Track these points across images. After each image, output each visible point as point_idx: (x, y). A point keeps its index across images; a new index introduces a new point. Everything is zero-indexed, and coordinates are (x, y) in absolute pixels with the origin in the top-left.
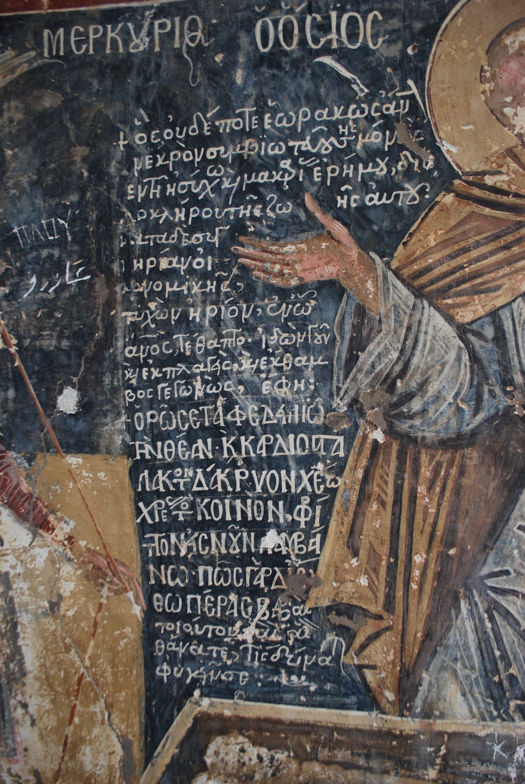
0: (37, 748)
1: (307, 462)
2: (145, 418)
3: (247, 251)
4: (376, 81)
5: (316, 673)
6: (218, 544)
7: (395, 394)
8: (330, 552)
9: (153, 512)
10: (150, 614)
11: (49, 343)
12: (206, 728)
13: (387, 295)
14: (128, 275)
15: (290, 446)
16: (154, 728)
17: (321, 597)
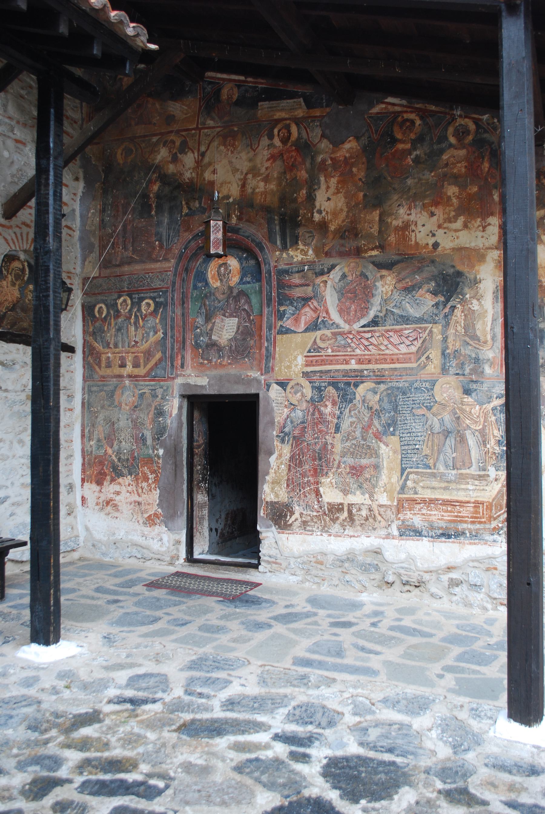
2: (401, 431)
3: (414, 410)
4: (428, 391)
6: (411, 447)
9: (402, 443)
10: (402, 457)
11: (389, 422)
13: (429, 415)
15: (419, 434)
16: (402, 475)
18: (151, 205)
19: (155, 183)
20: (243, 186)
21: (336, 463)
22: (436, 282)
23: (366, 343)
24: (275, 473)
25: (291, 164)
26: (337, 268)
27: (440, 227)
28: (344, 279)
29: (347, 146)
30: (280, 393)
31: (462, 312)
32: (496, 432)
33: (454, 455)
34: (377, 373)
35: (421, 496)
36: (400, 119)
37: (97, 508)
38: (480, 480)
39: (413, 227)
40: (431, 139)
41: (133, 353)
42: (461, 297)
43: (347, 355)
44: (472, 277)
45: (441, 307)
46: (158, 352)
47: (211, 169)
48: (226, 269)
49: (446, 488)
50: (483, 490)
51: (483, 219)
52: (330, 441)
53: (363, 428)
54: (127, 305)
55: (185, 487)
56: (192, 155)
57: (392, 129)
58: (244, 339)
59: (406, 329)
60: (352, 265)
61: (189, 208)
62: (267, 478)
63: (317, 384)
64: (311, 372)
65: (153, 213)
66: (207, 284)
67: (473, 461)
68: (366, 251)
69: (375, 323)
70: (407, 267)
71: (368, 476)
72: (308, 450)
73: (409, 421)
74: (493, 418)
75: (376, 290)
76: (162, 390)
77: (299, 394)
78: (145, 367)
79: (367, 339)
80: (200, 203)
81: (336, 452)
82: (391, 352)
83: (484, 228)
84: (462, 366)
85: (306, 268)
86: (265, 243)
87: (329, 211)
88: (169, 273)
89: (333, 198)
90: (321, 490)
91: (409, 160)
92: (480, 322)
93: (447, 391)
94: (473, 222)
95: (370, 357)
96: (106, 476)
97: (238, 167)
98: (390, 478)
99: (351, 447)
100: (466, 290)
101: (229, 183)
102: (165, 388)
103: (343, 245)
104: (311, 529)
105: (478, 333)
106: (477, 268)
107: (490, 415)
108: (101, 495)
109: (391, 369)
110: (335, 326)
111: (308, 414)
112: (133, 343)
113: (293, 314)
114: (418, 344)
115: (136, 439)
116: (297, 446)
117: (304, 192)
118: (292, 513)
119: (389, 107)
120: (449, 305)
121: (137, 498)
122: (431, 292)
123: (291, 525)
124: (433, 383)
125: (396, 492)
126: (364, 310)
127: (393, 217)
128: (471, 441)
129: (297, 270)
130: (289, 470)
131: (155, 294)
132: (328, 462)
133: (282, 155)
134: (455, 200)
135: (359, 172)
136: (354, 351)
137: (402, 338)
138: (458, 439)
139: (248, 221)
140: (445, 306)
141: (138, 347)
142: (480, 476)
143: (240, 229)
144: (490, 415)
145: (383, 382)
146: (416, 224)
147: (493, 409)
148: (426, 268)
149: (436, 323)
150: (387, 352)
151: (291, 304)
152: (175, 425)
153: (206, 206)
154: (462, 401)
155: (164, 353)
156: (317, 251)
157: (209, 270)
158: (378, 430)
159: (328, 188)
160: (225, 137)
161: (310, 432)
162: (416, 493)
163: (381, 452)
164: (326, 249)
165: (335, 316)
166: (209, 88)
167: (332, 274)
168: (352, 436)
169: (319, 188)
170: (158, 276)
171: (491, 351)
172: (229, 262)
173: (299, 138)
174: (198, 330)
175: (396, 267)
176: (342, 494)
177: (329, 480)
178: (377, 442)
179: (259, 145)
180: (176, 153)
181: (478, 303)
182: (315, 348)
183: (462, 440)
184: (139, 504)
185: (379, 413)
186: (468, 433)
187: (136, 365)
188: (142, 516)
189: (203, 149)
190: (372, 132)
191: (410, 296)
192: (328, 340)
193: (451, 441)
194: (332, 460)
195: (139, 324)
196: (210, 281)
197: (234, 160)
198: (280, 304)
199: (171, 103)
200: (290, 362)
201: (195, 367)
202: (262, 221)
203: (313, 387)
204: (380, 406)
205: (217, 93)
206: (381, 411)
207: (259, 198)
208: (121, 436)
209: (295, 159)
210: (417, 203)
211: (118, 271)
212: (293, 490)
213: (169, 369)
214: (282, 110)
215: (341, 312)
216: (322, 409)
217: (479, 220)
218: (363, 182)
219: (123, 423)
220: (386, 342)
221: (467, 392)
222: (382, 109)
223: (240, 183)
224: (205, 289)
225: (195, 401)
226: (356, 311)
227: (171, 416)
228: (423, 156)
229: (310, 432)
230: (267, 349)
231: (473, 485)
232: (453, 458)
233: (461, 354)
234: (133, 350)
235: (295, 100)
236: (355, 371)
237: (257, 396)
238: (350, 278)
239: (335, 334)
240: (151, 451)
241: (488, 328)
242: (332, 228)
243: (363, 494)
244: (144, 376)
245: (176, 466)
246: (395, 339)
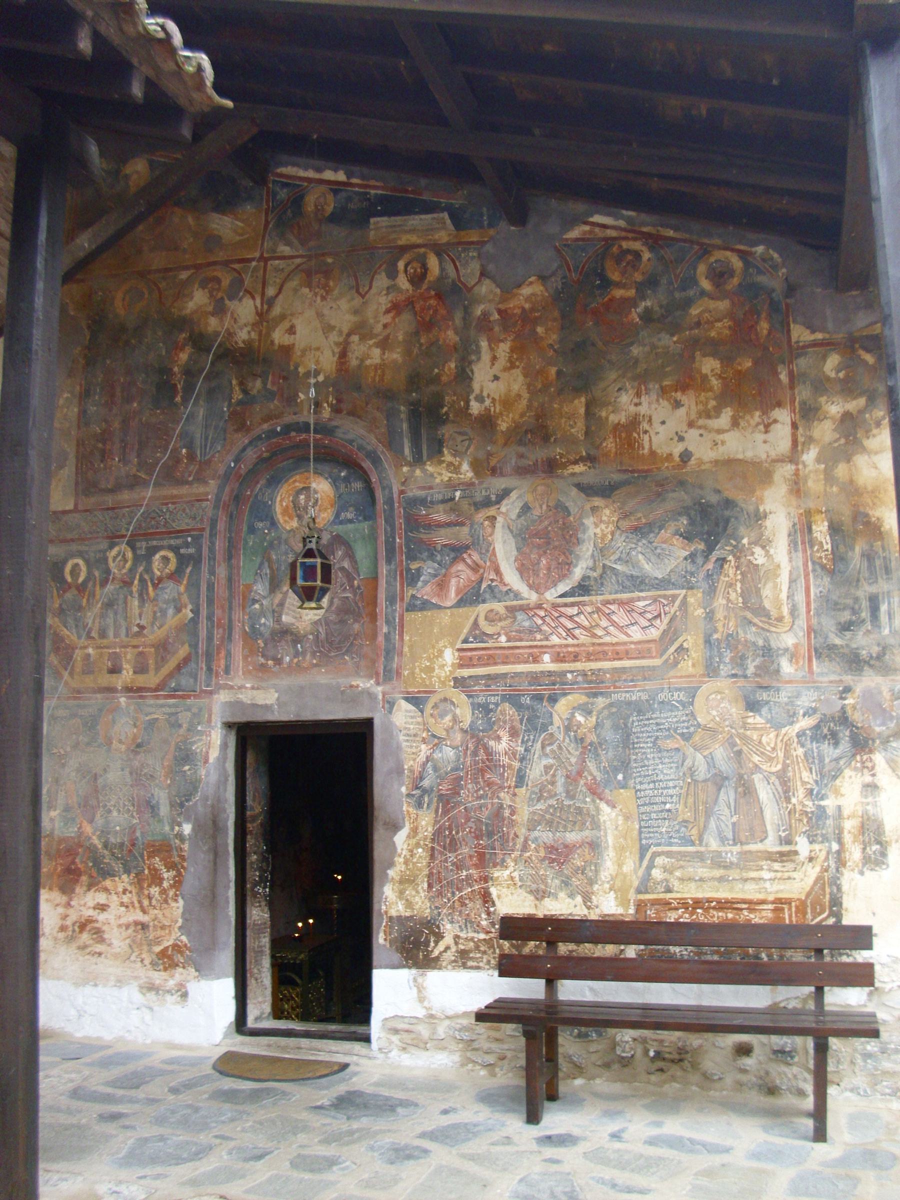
0: (611, 867)
1: (675, 787)
3: (659, 742)
5: (680, 838)
6: (656, 808)
7: (692, 771)
8: (680, 807)
10: (640, 827)
11: (615, 763)
12: (656, 855)
14: (634, 748)
16: (642, 858)
17: (680, 819)
18: (175, 385)
19: (182, 349)
20: (343, 355)
21: (521, 839)
22: (689, 515)
23: (570, 625)
24: (406, 863)
25: (427, 319)
26: (514, 495)
27: (691, 425)
29: (526, 291)
30: (412, 717)
31: (737, 568)
32: (806, 775)
33: (735, 819)
35: (679, 896)
36: (615, 249)
37: (61, 935)
38: (782, 861)
39: (645, 426)
40: (670, 283)
41: (135, 647)
42: (734, 543)
43: (536, 647)
44: (751, 508)
45: (700, 560)
46: (183, 644)
47: (286, 325)
48: (308, 498)
49: (721, 879)
50: (789, 878)
51: (765, 413)
52: (507, 801)
53: (567, 777)
54: (126, 561)
55: (231, 893)
56: (251, 302)
57: (602, 265)
58: (342, 622)
59: (639, 599)
60: (540, 489)
61: (245, 392)
62: (391, 873)
63: (481, 700)
64: (470, 677)
65: (178, 399)
66: (274, 524)
67: (769, 827)
68: (564, 466)
69: (583, 588)
71: (579, 863)
72: (468, 819)
73: (651, 762)
74: (800, 751)
75: (584, 532)
76: (189, 714)
77: (448, 717)
78: (156, 673)
79: (571, 618)
80: (265, 383)
81: (519, 820)
82: (615, 640)
83: (767, 428)
84: (740, 661)
85: (458, 494)
86: (383, 452)
87: (497, 398)
88: (204, 504)
89: (504, 376)
90: (494, 891)
91: (635, 316)
92: (770, 585)
93: (718, 706)
94: (748, 417)
95: (577, 649)
96: (80, 875)
97: (333, 323)
98: (620, 866)
99: (546, 811)
100: (742, 530)
101: (318, 349)
102: (194, 710)
103: (521, 456)
104: (475, 964)
105: (767, 604)
106: (758, 493)
107: (795, 745)
108: (71, 911)
109: (615, 670)
110: (512, 595)
111: (465, 754)
112: (136, 629)
113: (435, 576)
114: (662, 625)
115: (139, 806)
116: (446, 812)
117: (453, 365)
118: (439, 937)
119: (597, 230)
120: (713, 557)
121: (140, 916)
122: (681, 535)
123: (437, 958)
124: (692, 693)
125: (632, 891)
126: (564, 568)
127: (610, 408)
128: (765, 793)
129: (440, 497)
130: (432, 857)
131: (179, 542)
132: (504, 839)
133: (412, 303)
134: (715, 382)
135: (548, 333)
136: (547, 639)
137: (635, 615)
138: (740, 790)
139: (352, 413)
140: (706, 558)
141: (145, 636)
142: (782, 854)
143: (337, 427)
144: (795, 745)
145: (601, 693)
146: (650, 421)
147: (798, 735)
148: (671, 495)
149: (692, 588)
150: (607, 639)
151: (432, 557)
152: (214, 777)
153: (275, 389)
154: (745, 723)
155: (194, 646)
156: (476, 466)
157: (279, 499)
158: (594, 778)
159: (494, 359)
160: (309, 274)
161: (470, 786)
162: (669, 890)
163: (602, 819)
164: (492, 463)
165: (512, 578)
166: (283, 194)
168: (549, 791)
169: (479, 359)
170: (184, 510)
171: (791, 634)
172: (314, 485)
173: (442, 277)
174: (257, 606)
175: (618, 492)
176: (532, 898)
177: (507, 872)
178: (593, 801)
179: (370, 288)
180: (222, 298)
181: (763, 552)
183: (747, 791)
184: (144, 926)
185: (596, 748)
186: (757, 778)
187: (141, 669)
188: (150, 951)
189: (271, 292)
190: (569, 270)
191: (644, 541)
192: (500, 620)
193: (728, 795)
194: (512, 836)
195: (148, 594)
196: (280, 518)
197: (326, 311)
198: (412, 557)
199: (215, 216)
200: (429, 659)
201: (250, 672)
202: (378, 414)
203: (472, 704)
204: (598, 736)
205: (297, 201)
206: (600, 744)
207: (372, 374)
208: (109, 801)
209: (436, 311)
210: (651, 386)
211: (109, 500)
212: (440, 894)
213: (202, 676)
214: (412, 231)
215: (522, 570)
216: (492, 743)
217: (758, 413)
218: (555, 351)
219: (115, 775)
220: (604, 623)
221: (752, 706)
222: (585, 233)
223: (337, 350)
224: (269, 532)
225: (250, 736)
226: (549, 569)
227: (206, 761)
228: (656, 308)
229: (470, 786)
230: (387, 637)
231: (770, 870)
232: (734, 824)
233: (739, 641)
234: (135, 642)
235: (435, 215)
236: (550, 673)
237: (368, 723)
238: (537, 512)
239: (512, 610)
240: (167, 828)
241: (784, 595)
242: (503, 426)
243: (571, 896)
244: (156, 690)
245: (216, 854)
246: (621, 617)
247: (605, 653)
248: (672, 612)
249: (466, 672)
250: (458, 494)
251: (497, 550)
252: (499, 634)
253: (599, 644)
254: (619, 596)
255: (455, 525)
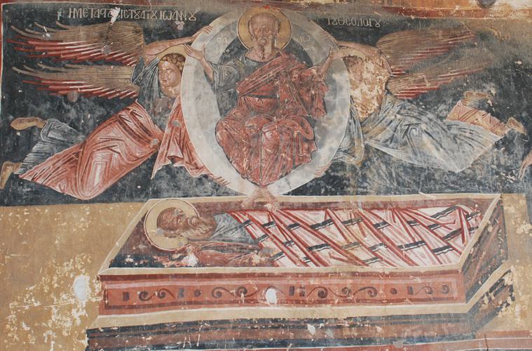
22: (498, 82)
23: (312, 241)
26: (216, 25)
28: (237, 55)
34: (347, 333)
43: (252, 275)
60: (261, 21)
69: (333, 181)
70: (417, 42)
75: (335, 92)
79: (314, 228)
82: (388, 269)
85: (115, 13)
95: (324, 282)
109: (392, 320)
110: (209, 185)
113: (64, 145)
114: (465, 245)
129: (83, 14)
136: (272, 263)
149: (510, 191)
150: (377, 267)
151: (58, 111)
165: (209, 156)
167: (200, 40)
175: (387, 38)
182: (140, 251)
191: (430, 115)
192: (186, 227)
200: (40, 295)
215: (230, 146)
220: (370, 240)
226: (276, 147)
236: (277, 324)
238: (254, 56)
239: (208, 211)
246: (397, 233)
247: (373, 290)
248: (482, 227)
249: (116, 320)
250: (115, 13)
251: (184, 108)
252: (184, 252)
253: (363, 275)
254: (393, 197)
255: (109, 63)
